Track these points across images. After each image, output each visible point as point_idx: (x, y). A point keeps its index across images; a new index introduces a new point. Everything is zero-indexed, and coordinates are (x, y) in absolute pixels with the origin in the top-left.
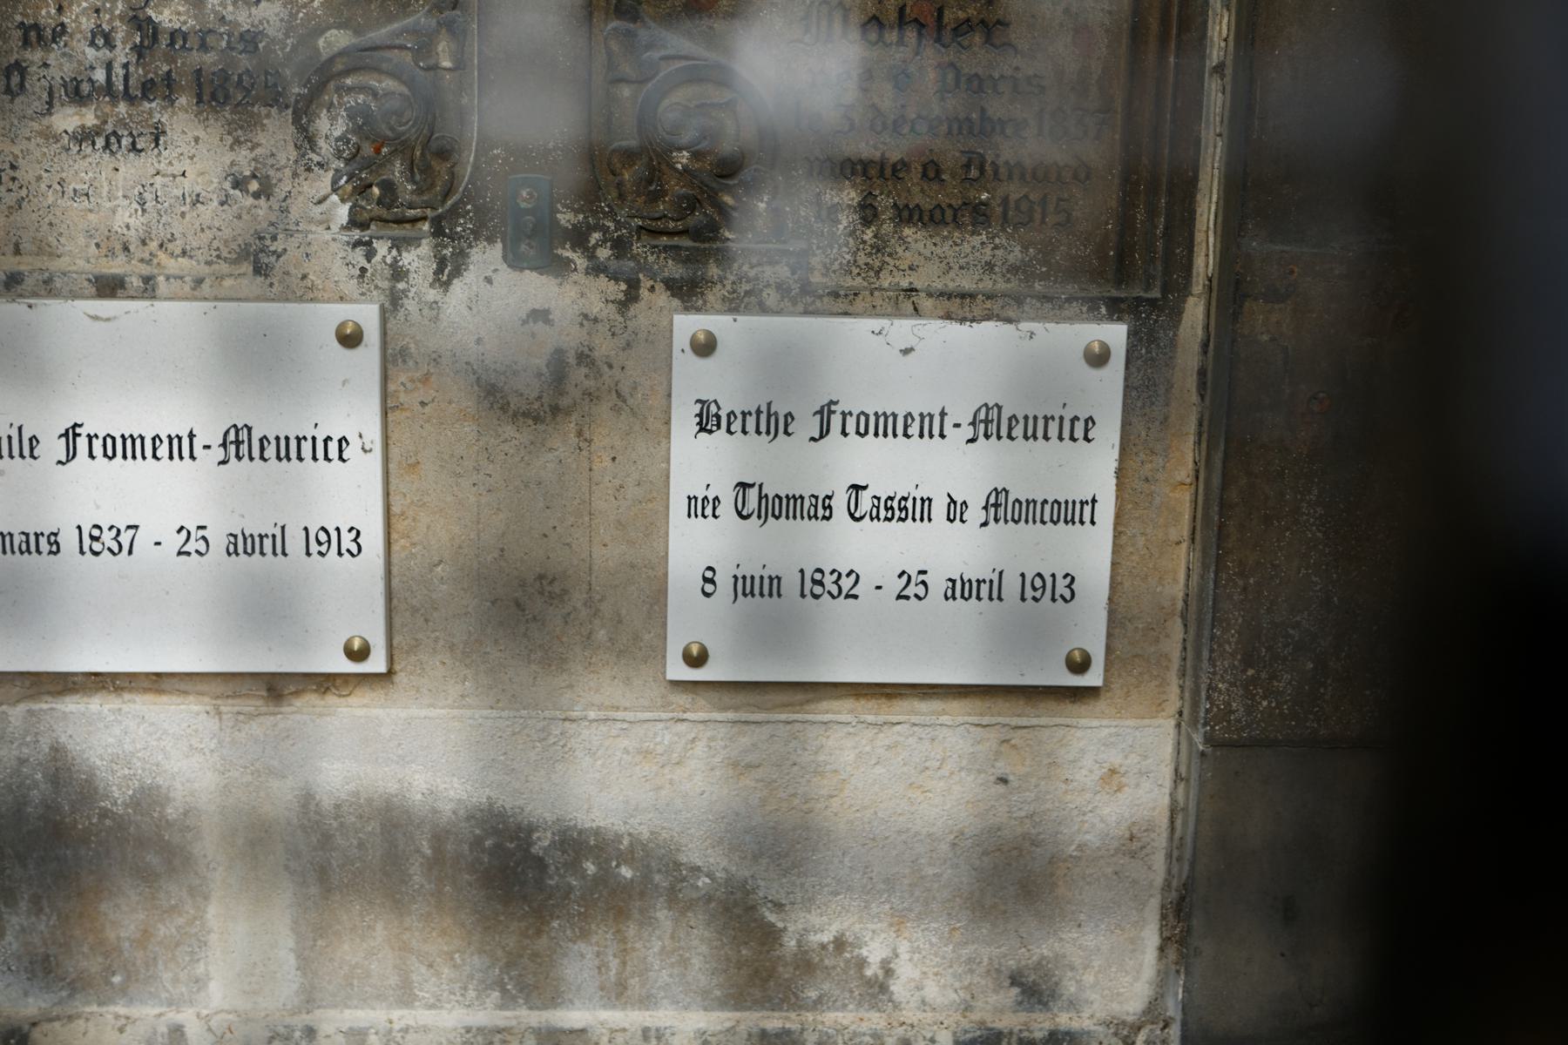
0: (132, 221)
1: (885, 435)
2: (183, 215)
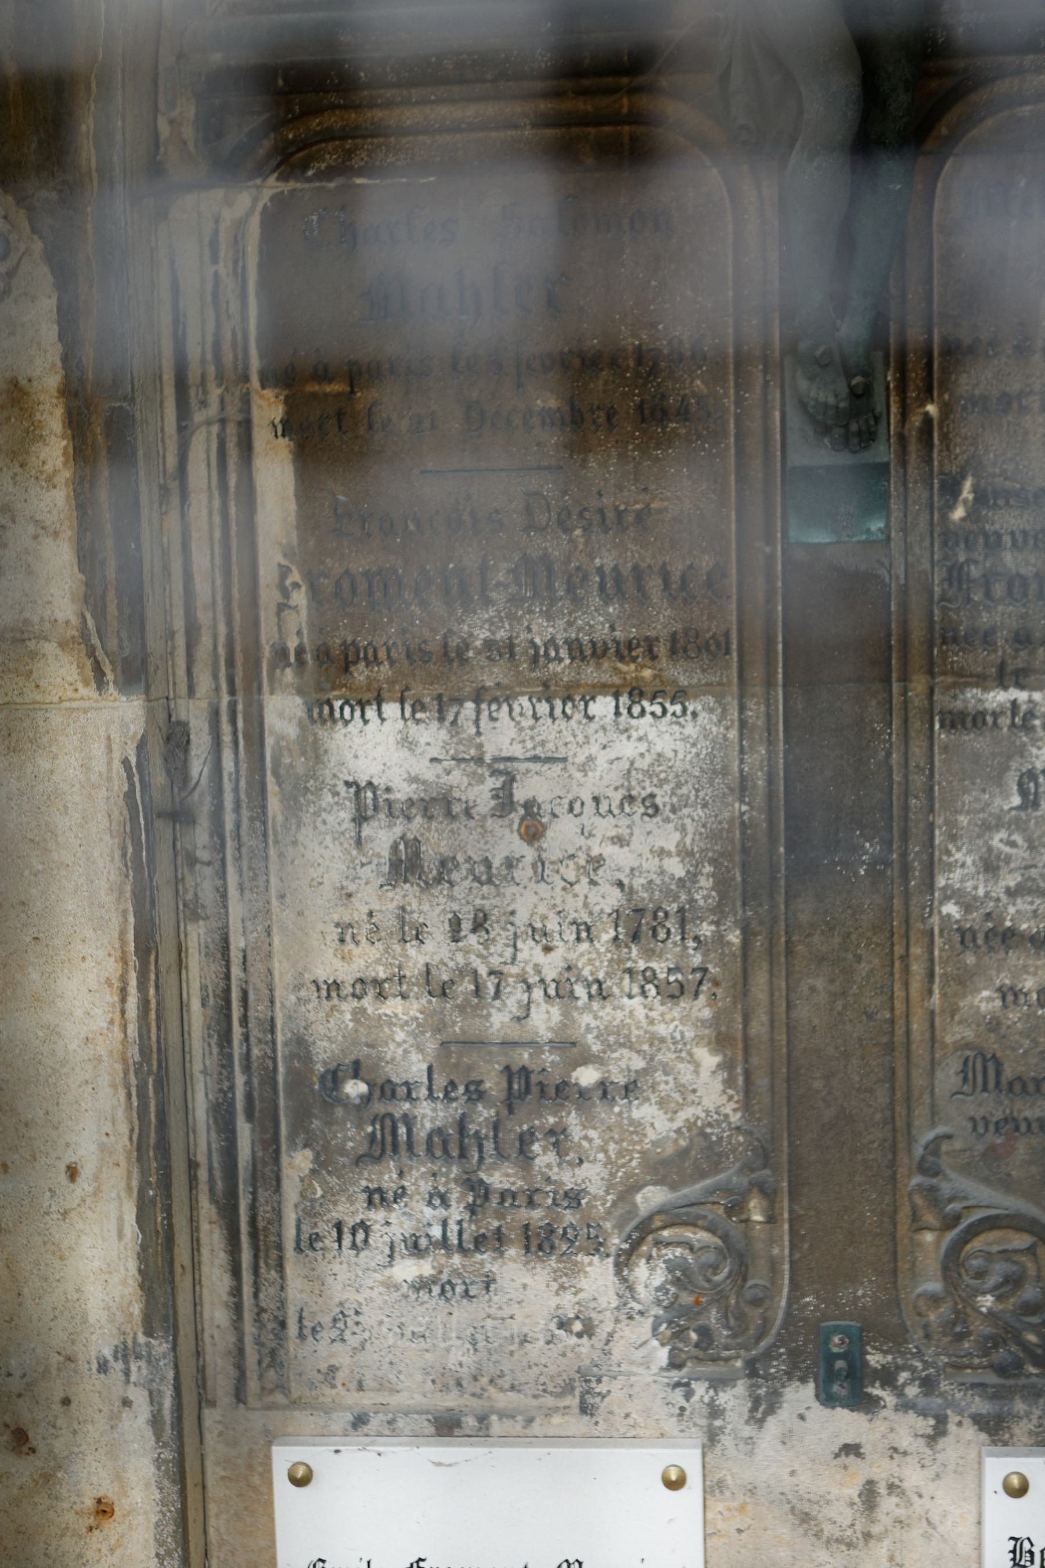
0: (464, 1359)
2: (512, 1353)
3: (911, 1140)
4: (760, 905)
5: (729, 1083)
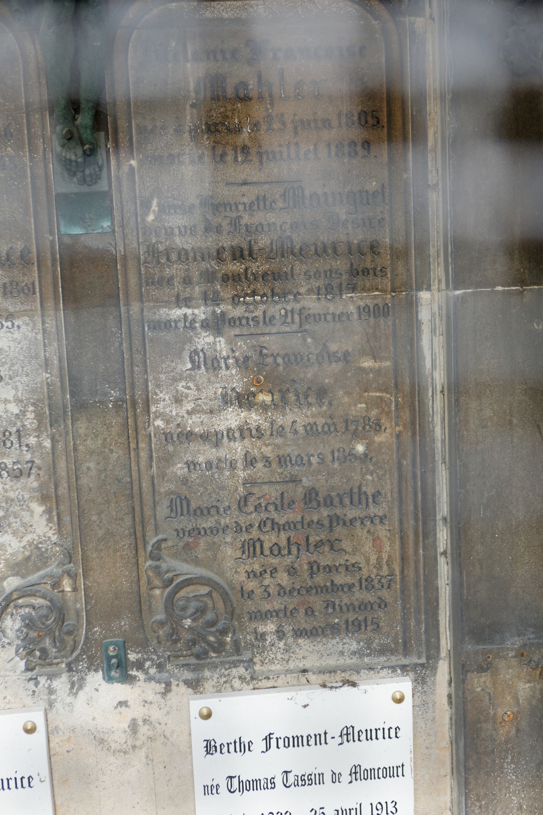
1: (298, 746)
3: (145, 543)
4: (60, 426)
5: (50, 520)
